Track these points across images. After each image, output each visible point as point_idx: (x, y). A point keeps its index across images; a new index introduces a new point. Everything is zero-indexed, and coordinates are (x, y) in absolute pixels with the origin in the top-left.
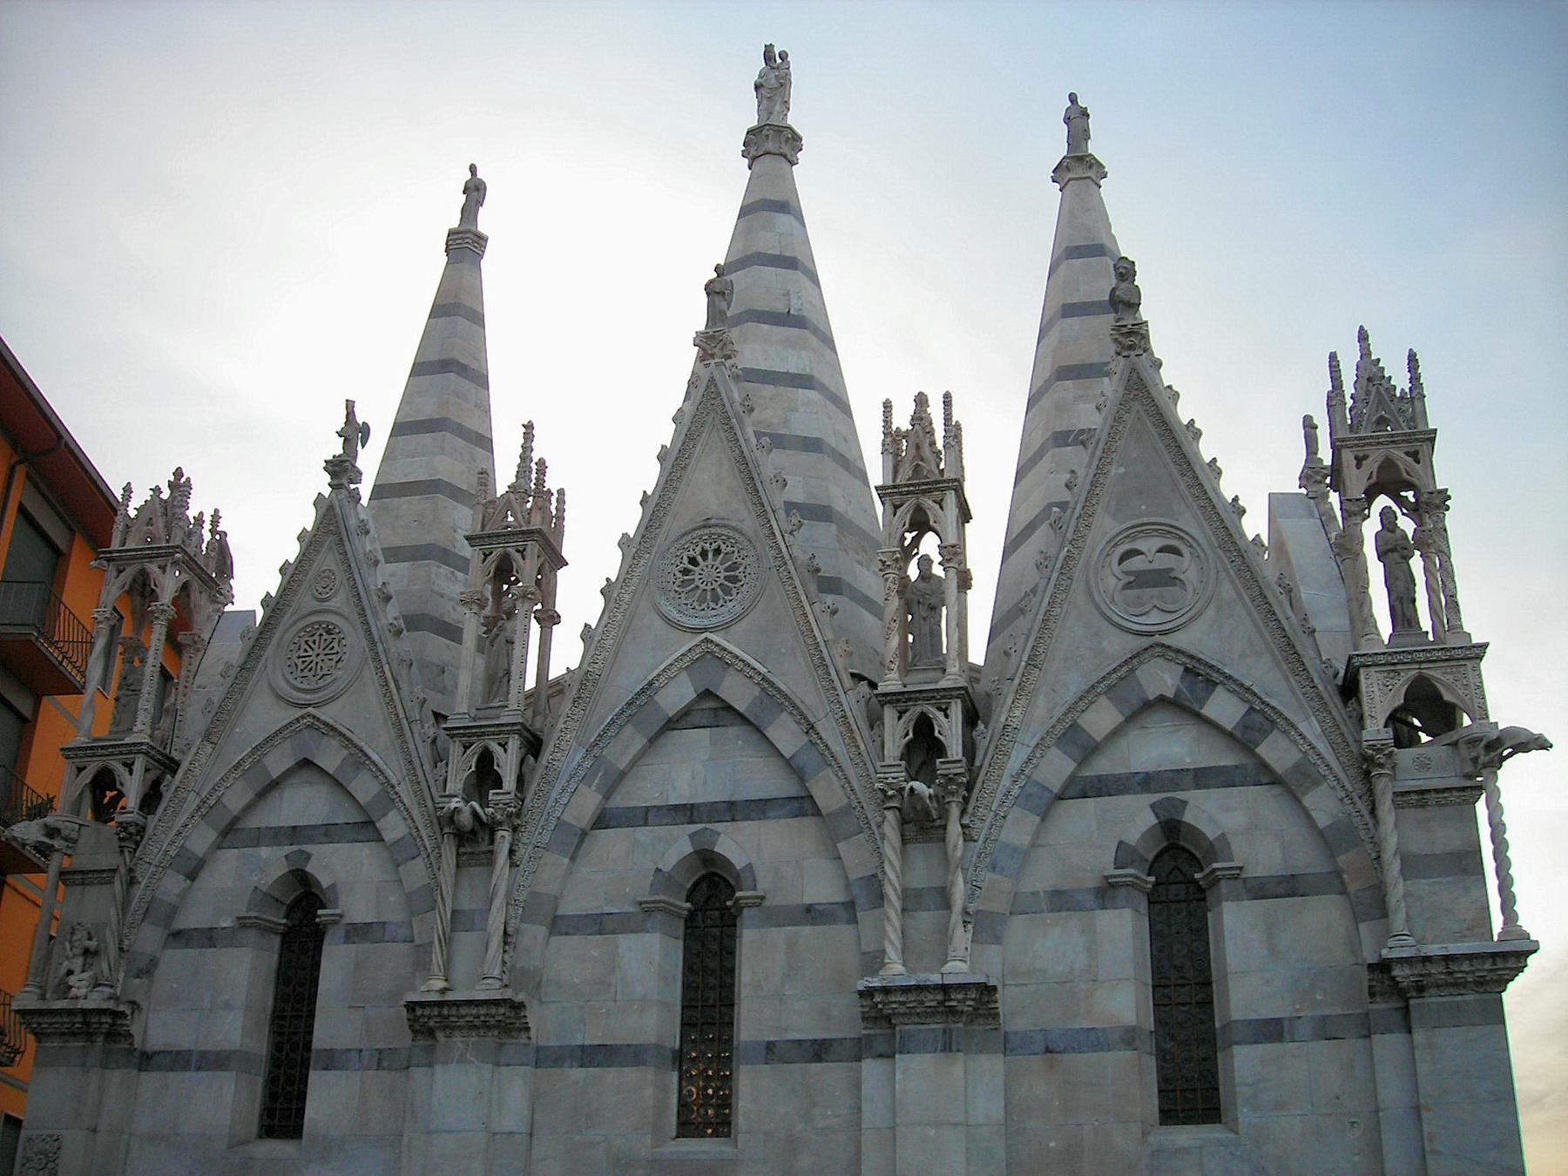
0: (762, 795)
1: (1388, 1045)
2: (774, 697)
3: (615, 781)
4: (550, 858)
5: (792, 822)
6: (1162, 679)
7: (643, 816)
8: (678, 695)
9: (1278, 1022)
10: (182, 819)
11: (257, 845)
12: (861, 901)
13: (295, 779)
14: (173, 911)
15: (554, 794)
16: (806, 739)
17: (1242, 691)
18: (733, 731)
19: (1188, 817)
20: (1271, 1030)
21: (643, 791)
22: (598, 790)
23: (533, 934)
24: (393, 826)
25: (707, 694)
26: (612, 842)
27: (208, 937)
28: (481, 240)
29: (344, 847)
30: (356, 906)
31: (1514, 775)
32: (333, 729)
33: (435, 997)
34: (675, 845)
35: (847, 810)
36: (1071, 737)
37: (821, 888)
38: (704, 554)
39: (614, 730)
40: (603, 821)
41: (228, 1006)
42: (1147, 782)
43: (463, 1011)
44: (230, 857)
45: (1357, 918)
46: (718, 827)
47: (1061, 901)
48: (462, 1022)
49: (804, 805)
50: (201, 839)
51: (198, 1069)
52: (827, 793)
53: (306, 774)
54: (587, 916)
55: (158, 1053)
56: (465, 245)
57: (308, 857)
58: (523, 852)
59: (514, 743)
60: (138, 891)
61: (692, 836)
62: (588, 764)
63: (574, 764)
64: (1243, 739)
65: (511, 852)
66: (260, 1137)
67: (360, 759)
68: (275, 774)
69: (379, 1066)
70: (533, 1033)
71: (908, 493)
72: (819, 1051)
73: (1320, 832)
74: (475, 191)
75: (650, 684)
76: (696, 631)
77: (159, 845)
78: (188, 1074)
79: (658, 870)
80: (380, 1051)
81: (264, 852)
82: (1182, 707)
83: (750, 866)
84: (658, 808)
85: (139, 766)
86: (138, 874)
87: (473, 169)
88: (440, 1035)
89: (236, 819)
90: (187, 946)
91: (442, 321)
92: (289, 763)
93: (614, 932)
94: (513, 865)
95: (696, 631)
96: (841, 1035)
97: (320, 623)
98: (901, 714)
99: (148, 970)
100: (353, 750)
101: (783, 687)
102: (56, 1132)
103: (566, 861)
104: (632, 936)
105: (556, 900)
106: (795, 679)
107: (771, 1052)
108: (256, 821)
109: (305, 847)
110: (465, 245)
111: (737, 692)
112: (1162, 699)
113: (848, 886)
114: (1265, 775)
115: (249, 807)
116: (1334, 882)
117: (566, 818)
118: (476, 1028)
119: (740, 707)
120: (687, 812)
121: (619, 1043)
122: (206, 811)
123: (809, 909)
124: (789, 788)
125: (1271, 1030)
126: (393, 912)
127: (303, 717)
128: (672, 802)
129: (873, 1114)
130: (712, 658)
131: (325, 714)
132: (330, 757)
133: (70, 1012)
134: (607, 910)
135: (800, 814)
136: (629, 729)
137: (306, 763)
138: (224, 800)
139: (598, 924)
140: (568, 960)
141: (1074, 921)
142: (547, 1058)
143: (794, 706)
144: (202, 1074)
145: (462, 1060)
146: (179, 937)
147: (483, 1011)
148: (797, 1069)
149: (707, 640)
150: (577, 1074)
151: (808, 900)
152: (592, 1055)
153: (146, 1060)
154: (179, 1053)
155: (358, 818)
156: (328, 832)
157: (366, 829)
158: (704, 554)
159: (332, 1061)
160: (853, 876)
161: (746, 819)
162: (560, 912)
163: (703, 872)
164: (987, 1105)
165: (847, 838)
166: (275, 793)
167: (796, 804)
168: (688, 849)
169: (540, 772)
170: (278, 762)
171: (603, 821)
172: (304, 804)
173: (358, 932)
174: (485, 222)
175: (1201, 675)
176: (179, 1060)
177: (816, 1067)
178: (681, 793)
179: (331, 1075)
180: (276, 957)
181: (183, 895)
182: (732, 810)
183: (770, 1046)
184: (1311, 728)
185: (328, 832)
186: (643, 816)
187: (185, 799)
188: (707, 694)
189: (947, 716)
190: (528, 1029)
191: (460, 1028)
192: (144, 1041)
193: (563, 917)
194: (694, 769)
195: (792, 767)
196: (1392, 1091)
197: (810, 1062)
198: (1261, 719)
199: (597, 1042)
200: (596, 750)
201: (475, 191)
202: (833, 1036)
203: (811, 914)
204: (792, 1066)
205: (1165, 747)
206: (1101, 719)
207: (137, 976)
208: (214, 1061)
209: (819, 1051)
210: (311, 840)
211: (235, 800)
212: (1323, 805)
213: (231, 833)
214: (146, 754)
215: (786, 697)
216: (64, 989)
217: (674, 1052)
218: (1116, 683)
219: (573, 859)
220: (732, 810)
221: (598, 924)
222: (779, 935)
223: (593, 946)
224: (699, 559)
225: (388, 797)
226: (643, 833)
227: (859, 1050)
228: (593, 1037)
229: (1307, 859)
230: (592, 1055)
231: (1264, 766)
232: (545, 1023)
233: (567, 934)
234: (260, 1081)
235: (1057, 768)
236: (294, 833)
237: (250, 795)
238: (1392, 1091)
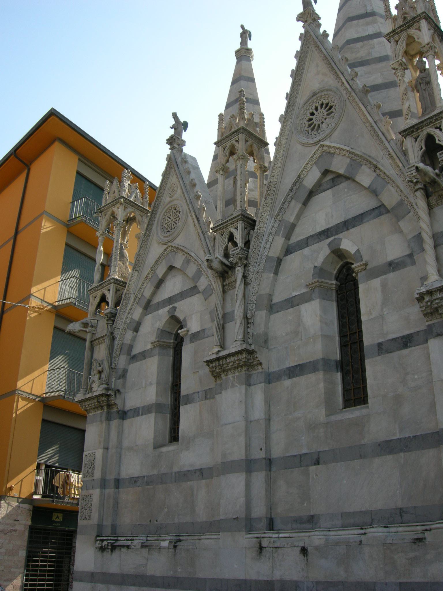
0: (361, 212)
2: (357, 160)
4: (265, 276)
5: (376, 220)
7: (306, 243)
8: (312, 177)
10: (129, 307)
11: (158, 310)
13: (169, 277)
14: (131, 347)
15: (263, 244)
16: (374, 174)
18: (344, 186)
22: (282, 237)
23: (261, 316)
28: (249, 51)
30: (194, 326)
32: (178, 249)
33: (214, 356)
34: (321, 252)
35: (400, 204)
37: (395, 249)
38: (316, 109)
39: (286, 205)
41: (151, 384)
43: (228, 360)
44: (149, 318)
46: (340, 236)
48: (229, 367)
49: (380, 210)
50: (137, 314)
51: (142, 415)
53: (173, 272)
54: (286, 300)
55: (128, 411)
56: (244, 55)
57: (175, 309)
58: (251, 277)
59: (240, 225)
60: (116, 342)
61: (329, 245)
62: (276, 225)
63: (270, 227)
65: (244, 277)
66: (170, 442)
68: (160, 276)
69: (206, 398)
70: (264, 365)
71: (401, 31)
72: (406, 342)
74: (245, 35)
75: (299, 177)
76: (315, 144)
77: (121, 321)
78: (139, 417)
79: (315, 267)
80: (206, 391)
81: (161, 311)
83: (358, 251)
84: (312, 236)
86: (115, 334)
87: (242, 27)
88: (223, 375)
89: (149, 301)
90: (137, 361)
91: (235, 85)
92: (164, 270)
93: (298, 305)
94: (246, 284)
95: (315, 144)
96: (417, 329)
97: (171, 206)
98: (416, 139)
99: (124, 375)
100: (186, 255)
101: (359, 153)
102: (93, 451)
103: (272, 275)
104: (306, 304)
105: (270, 296)
106: (367, 146)
107: (381, 348)
109: (175, 305)
110: (244, 55)
111: (339, 165)
115: (154, 294)
117: (270, 255)
118: (236, 368)
119: (341, 171)
120: (325, 233)
121: (305, 361)
122: (137, 300)
124: (372, 203)
127: (167, 248)
128: (319, 230)
132: (178, 261)
134: (294, 294)
135: (381, 214)
136: (293, 202)
138: (144, 294)
140: (279, 325)
143: (366, 160)
144: (144, 417)
145: (233, 386)
146: (134, 358)
147: (236, 358)
148: (395, 355)
149: (322, 146)
150: (287, 383)
151: (390, 258)
152: (295, 371)
154: (136, 409)
156: (182, 295)
158: (316, 109)
159: (189, 400)
161: (354, 226)
162: (273, 302)
163: (341, 263)
165: (403, 217)
166: (163, 285)
167: (377, 211)
168: (327, 251)
169: (255, 235)
170: (161, 271)
171: (288, 251)
173: (196, 337)
174: (250, 44)
176: (137, 412)
178: (321, 225)
179: (188, 407)
180: (171, 358)
181: (134, 339)
182: (347, 225)
183: (380, 345)
185: (182, 295)
186: (306, 243)
187: (130, 298)
188: (326, 172)
189: (441, 130)
190: (261, 364)
191: (230, 369)
192: (124, 406)
193: (275, 304)
194: (325, 212)
195: (374, 192)
197: (401, 349)
199: (295, 364)
200: (279, 218)
201: (245, 35)
202: (412, 331)
203: (393, 266)
204: (392, 354)
207: (119, 379)
208: (146, 410)
209: (406, 342)
210: (176, 301)
211: (147, 294)
213: (148, 307)
214: (114, 283)
215: (361, 157)
217: (336, 362)
219: (276, 273)
220: (347, 225)
221: (292, 303)
222: (376, 282)
223: (289, 314)
224: (315, 112)
226: (306, 251)
230: (295, 371)
232: (272, 360)
233: (278, 312)
234: (168, 416)
236: (171, 300)
237: (153, 288)
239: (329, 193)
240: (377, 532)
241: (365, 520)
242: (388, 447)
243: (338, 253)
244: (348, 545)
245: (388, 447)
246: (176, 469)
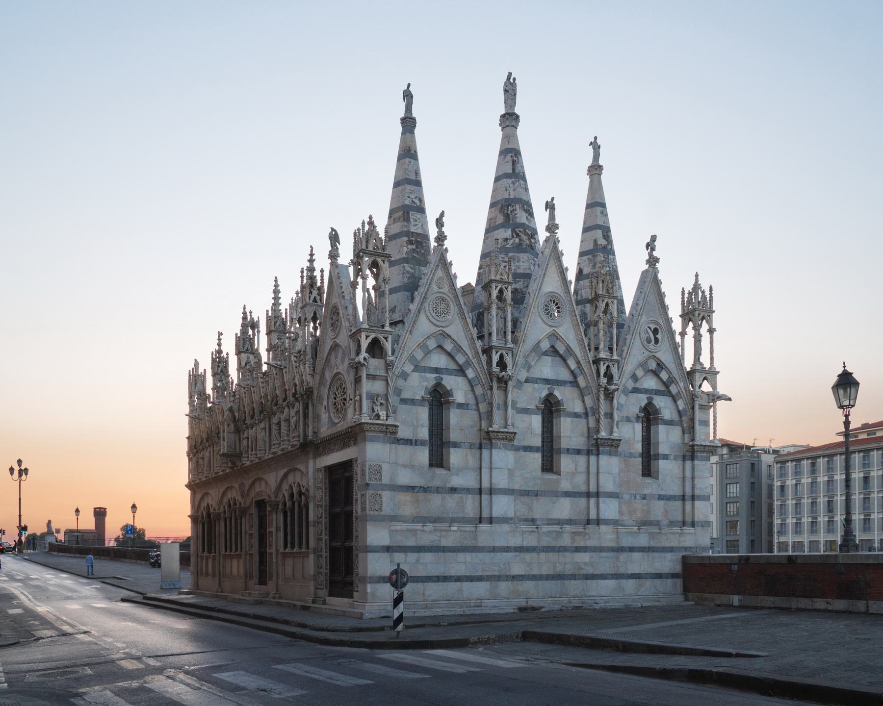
1: (688, 463)
3: (529, 368)
6: (653, 365)
8: (545, 345)
9: (667, 455)
12: (590, 414)
17: (669, 372)
18: (558, 358)
19: (654, 402)
20: (666, 457)
21: (536, 373)
24: (470, 373)
25: (552, 347)
26: (529, 387)
27: (412, 402)
29: (453, 377)
30: (459, 396)
31: (720, 404)
36: (634, 378)
37: (578, 408)
40: (527, 381)
42: (646, 391)
45: (684, 433)
47: (628, 419)
49: (575, 383)
50: (409, 368)
52: (581, 381)
57: (442, 379)
64: (666, 385)
67: (459, 348)
72: (578, 452)
73: (679, 411)
77: (397, 369)
81: (427, 375)
82: (656, 373)
85: (390, 339)
108: (422, 364)
111: (561, 349)
112: (652, 371)
113: (586, 409)
114: (669, 393)
116: (680, 423)
120: (547, 381)
123: (576, 413)
125: (666, 457)
126: (472, 401)
129: (593, 469)
130: (554, 336)
131: (447, 330)
132: (449, 347)
133: (383, 425)
137: (440, 347)
139: (526, 411)
141: (630, 425)
142: (517, 449)
146: (404, 401)
150: (523, 453)
151: (576, 411)
153: (398, 441)
155: (455, 367)
156: (448, 372)
157: (461, 371)
160: (588, 406)
164: (615, 470)
172: (439, 360)
175: (661, 365)
177: (577, 456)
183: (568, 449)
184: (682, 384)
185: (448, 372)
196: (688, 474)
198: (672, 380)
203: (576, 415)
205: (651, 383)
206: (640, 373)
208: (422, 443)
209: (578, 452)
212: (681, 404)
216: (378, 417)
218: (643, 365)
221: (526, 411)
222: (569, 420)
223: (526, 417)
225: (468, 363)
227: (589, 453)
228: (527, 444)
229: (675, 417)
231: (669, 392)
235: (630, 385)
236: (437, 370)
238: (688, 474)
239: (550, 358)
240: (568, 528)
241: (559, 522)
242: (567, 494)
243: (551, 395)
244: (557, 532)
245: (567, 494)
246: (449, 485)
